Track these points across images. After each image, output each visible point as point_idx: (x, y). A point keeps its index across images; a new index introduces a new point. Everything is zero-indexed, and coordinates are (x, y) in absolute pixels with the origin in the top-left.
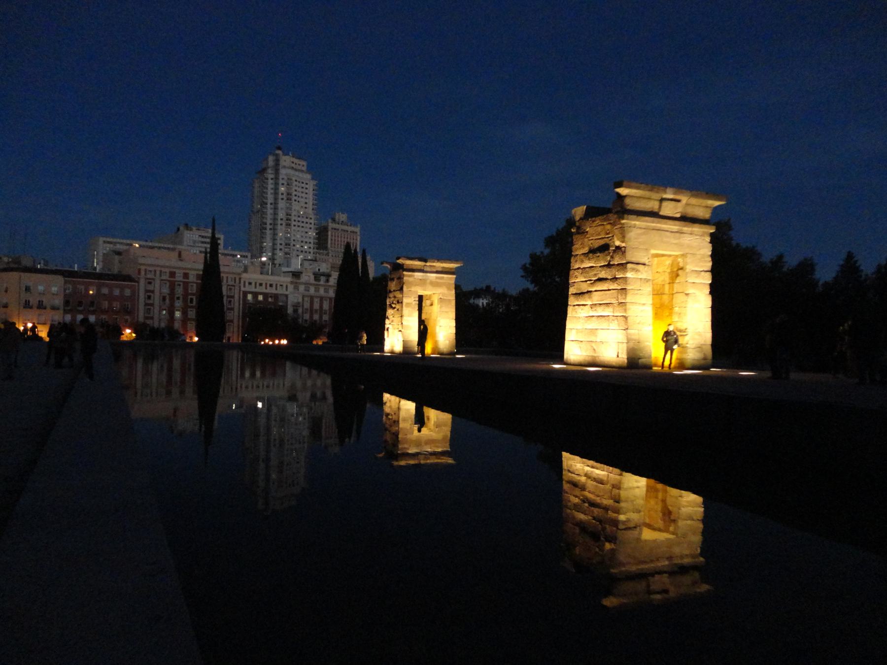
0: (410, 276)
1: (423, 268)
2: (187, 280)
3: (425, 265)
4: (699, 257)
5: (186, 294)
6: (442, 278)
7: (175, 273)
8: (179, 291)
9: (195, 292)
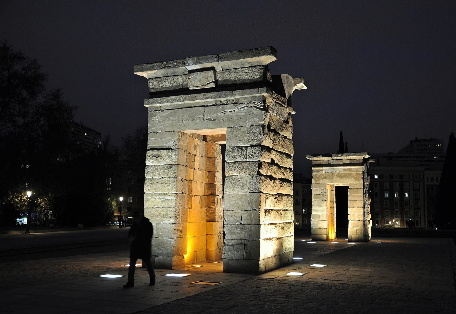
0: (317, 171)
1: (330, 163)
2: (402, 180)
3: (332, 160)
4: (245, 129)
6: (350, 170)
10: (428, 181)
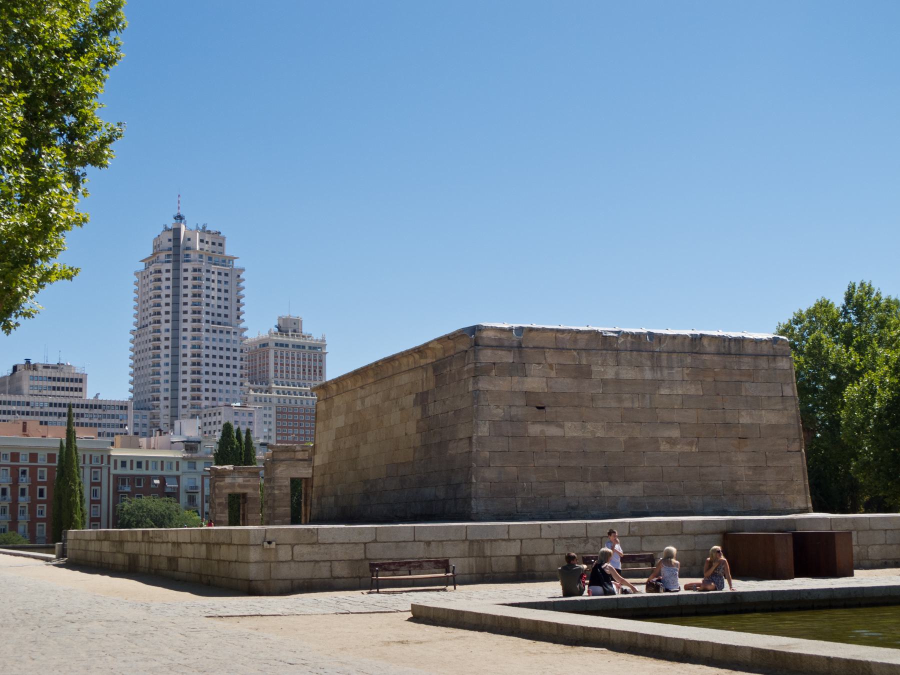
5: (34, 483)
7: (18, 454)
8: (24, 483)
9: (45, 480)
10: (115, 468)
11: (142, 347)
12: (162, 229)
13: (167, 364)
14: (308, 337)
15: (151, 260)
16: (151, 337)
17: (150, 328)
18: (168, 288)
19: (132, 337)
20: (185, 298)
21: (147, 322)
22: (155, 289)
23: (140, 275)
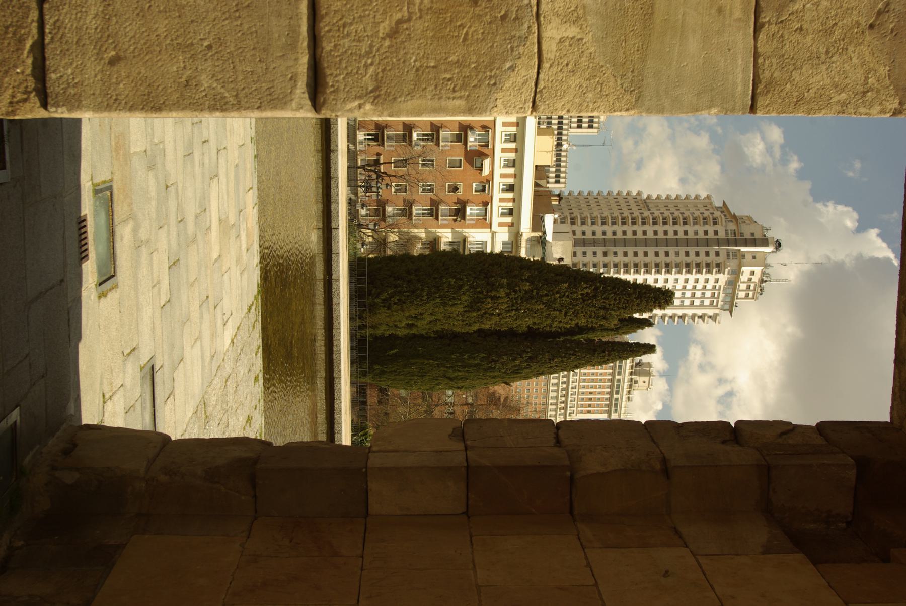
10: (505, 124)
11: (623, 205)
12: (766, 225)
13: (604, 234)
14: (629, 398)
15: (726, 213)
16: (636, 214)
17: (646, 214)
18: (696, 233)
19: (634, 193)
20: (684, 254)
21: (653, 210)
22: (695, 219)
23: (707, 201)
